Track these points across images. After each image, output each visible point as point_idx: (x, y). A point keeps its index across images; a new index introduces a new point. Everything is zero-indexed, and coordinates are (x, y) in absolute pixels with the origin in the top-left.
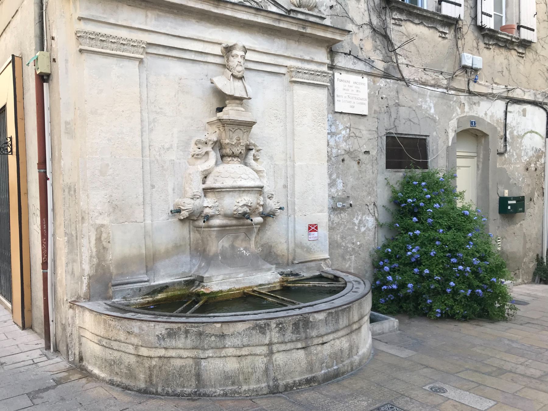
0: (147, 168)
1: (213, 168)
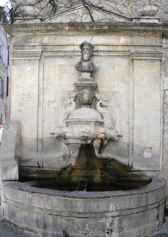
0: (40, 111)
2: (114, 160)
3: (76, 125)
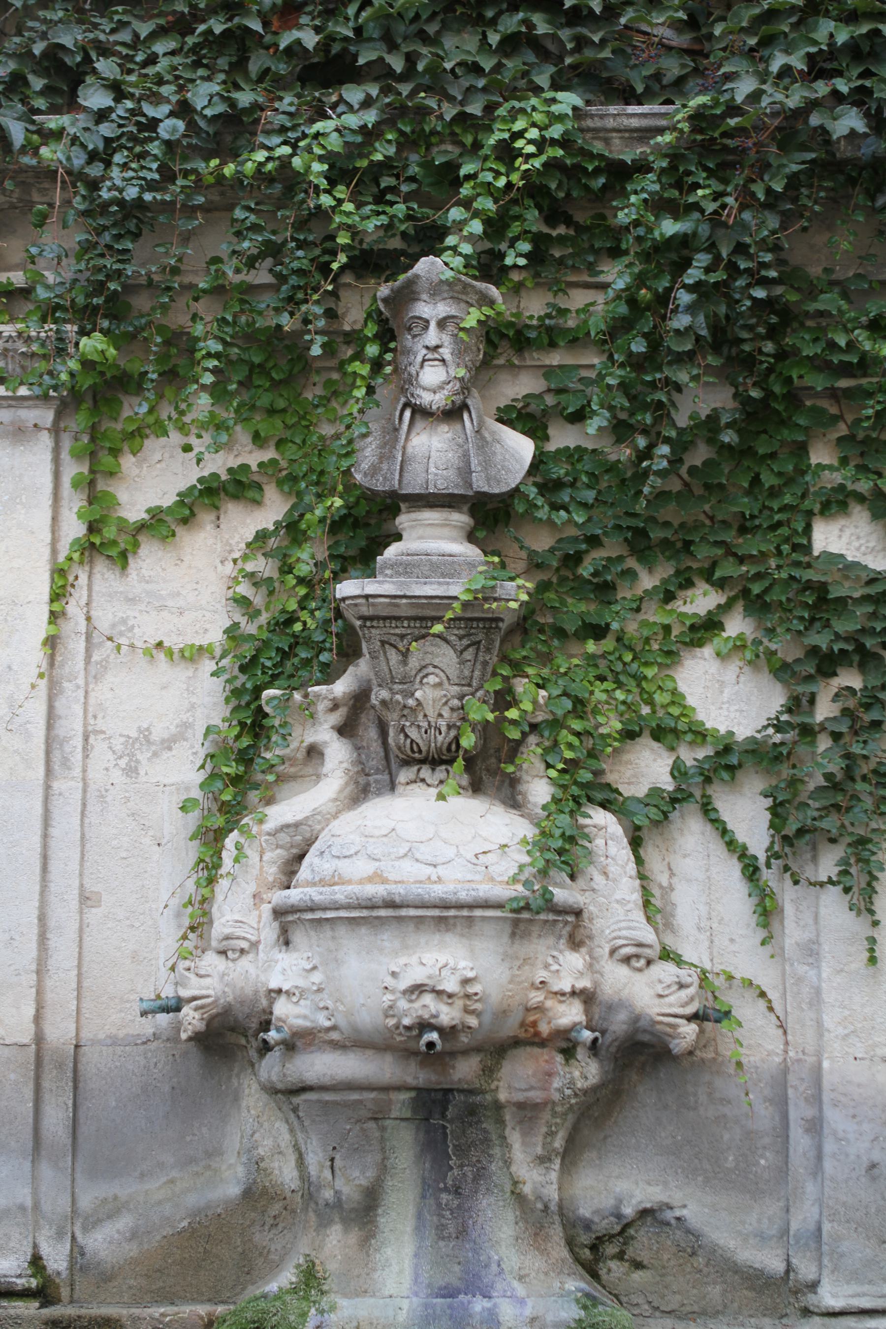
0: (66, 824)
2: (669, 1215)
3: (363, 930)
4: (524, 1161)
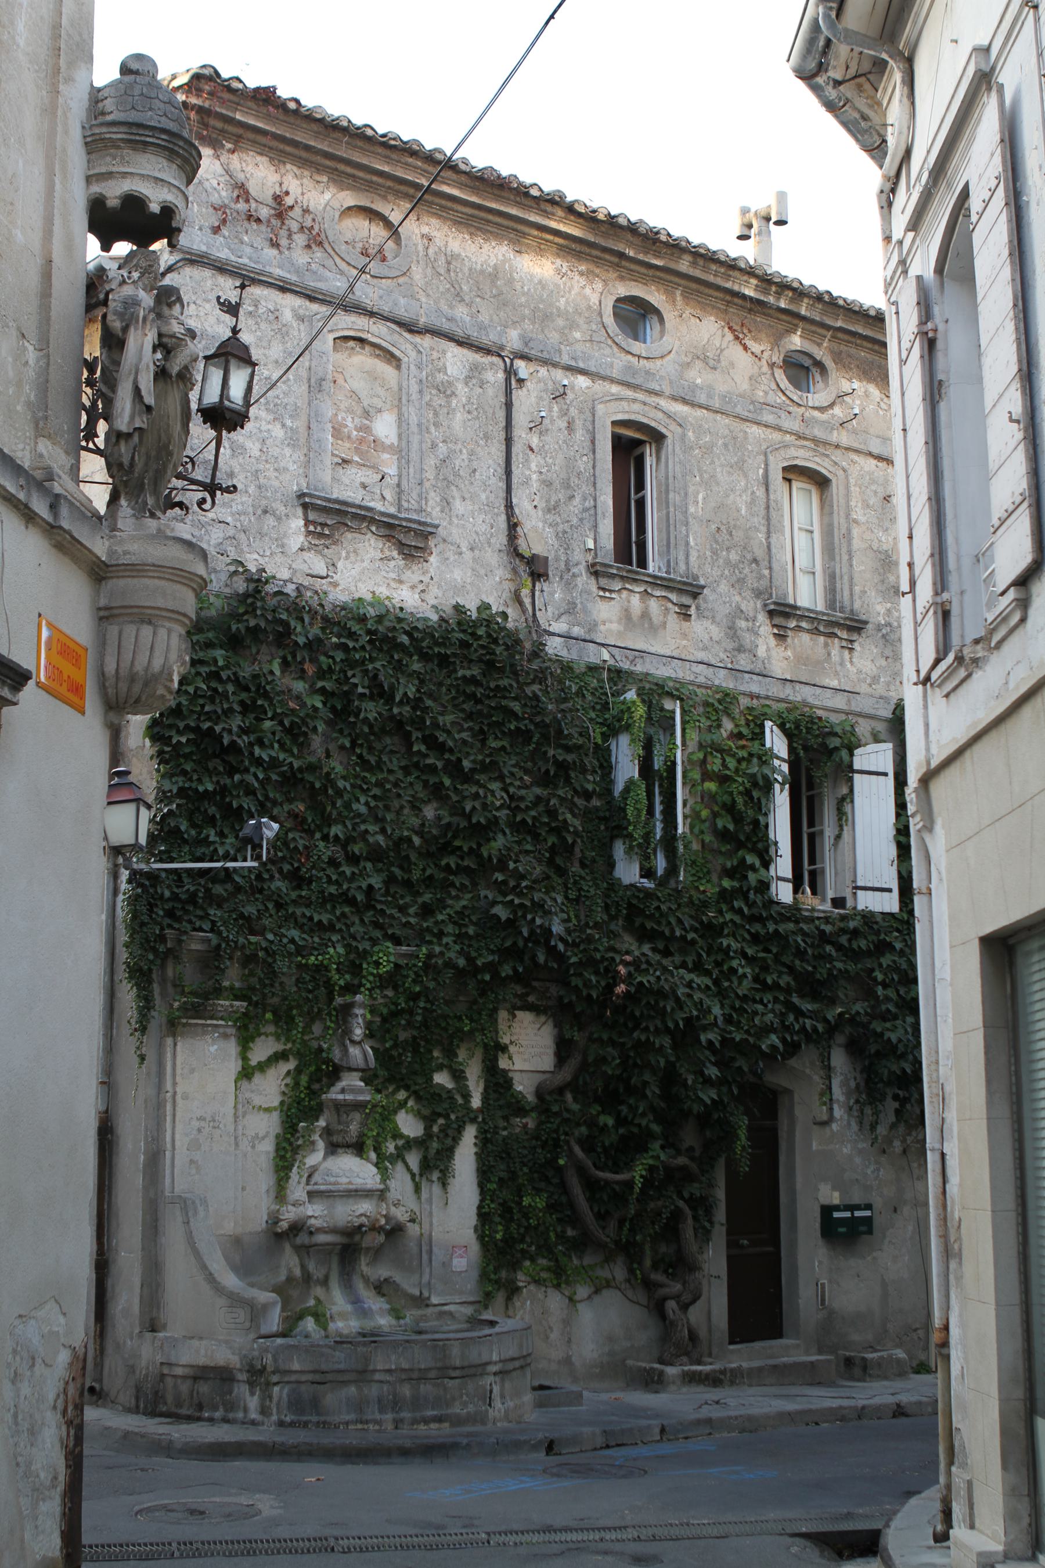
1: (320, 1164)
4: (363, 1265)
